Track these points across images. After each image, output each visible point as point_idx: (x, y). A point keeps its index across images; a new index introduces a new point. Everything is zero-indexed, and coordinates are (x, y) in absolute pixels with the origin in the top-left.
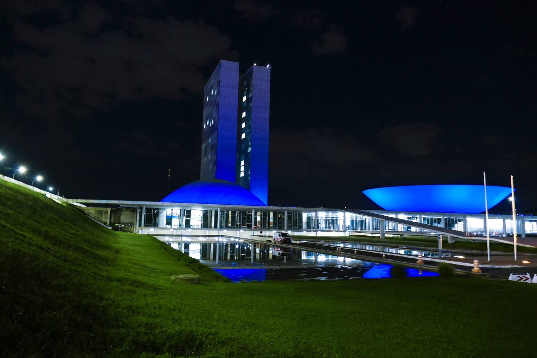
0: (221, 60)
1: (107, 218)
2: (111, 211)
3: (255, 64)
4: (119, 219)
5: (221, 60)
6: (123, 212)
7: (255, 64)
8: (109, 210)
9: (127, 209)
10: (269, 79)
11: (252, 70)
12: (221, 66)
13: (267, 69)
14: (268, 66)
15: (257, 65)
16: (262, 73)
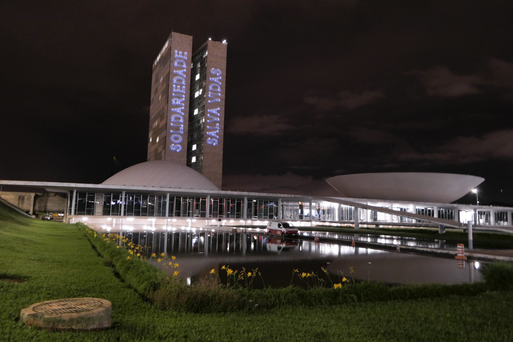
0: (173, 33)
1: (30, 205)
2: (36, 197)
4: (46, 206)
5: (173, 33)
6: (50, 198)
7: (210, 39)
8: (33, 195)
9: (56, 194)
10: (226, 56)
11: (207, 46)
12: (173, 39)
13: (223, 45)
14: (224, 42)
15: (212, 40)
16: (217, 50)
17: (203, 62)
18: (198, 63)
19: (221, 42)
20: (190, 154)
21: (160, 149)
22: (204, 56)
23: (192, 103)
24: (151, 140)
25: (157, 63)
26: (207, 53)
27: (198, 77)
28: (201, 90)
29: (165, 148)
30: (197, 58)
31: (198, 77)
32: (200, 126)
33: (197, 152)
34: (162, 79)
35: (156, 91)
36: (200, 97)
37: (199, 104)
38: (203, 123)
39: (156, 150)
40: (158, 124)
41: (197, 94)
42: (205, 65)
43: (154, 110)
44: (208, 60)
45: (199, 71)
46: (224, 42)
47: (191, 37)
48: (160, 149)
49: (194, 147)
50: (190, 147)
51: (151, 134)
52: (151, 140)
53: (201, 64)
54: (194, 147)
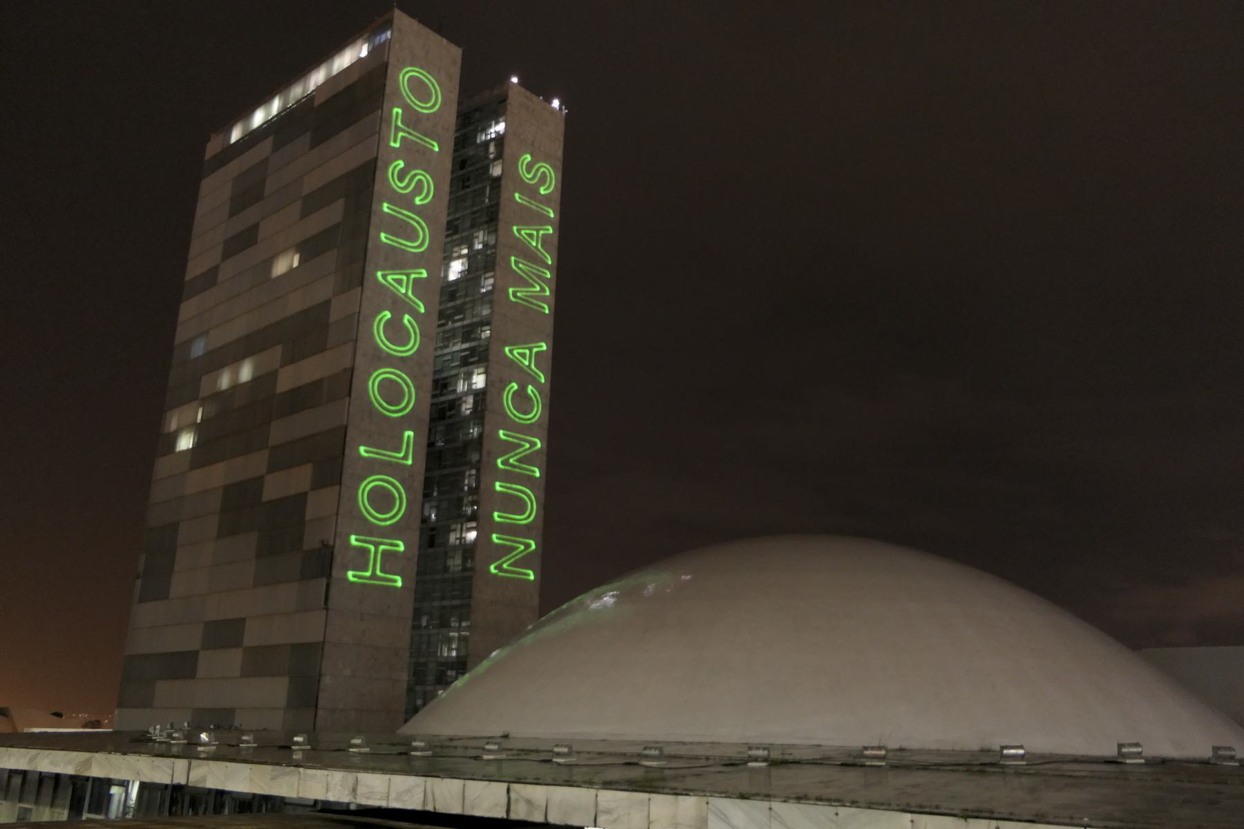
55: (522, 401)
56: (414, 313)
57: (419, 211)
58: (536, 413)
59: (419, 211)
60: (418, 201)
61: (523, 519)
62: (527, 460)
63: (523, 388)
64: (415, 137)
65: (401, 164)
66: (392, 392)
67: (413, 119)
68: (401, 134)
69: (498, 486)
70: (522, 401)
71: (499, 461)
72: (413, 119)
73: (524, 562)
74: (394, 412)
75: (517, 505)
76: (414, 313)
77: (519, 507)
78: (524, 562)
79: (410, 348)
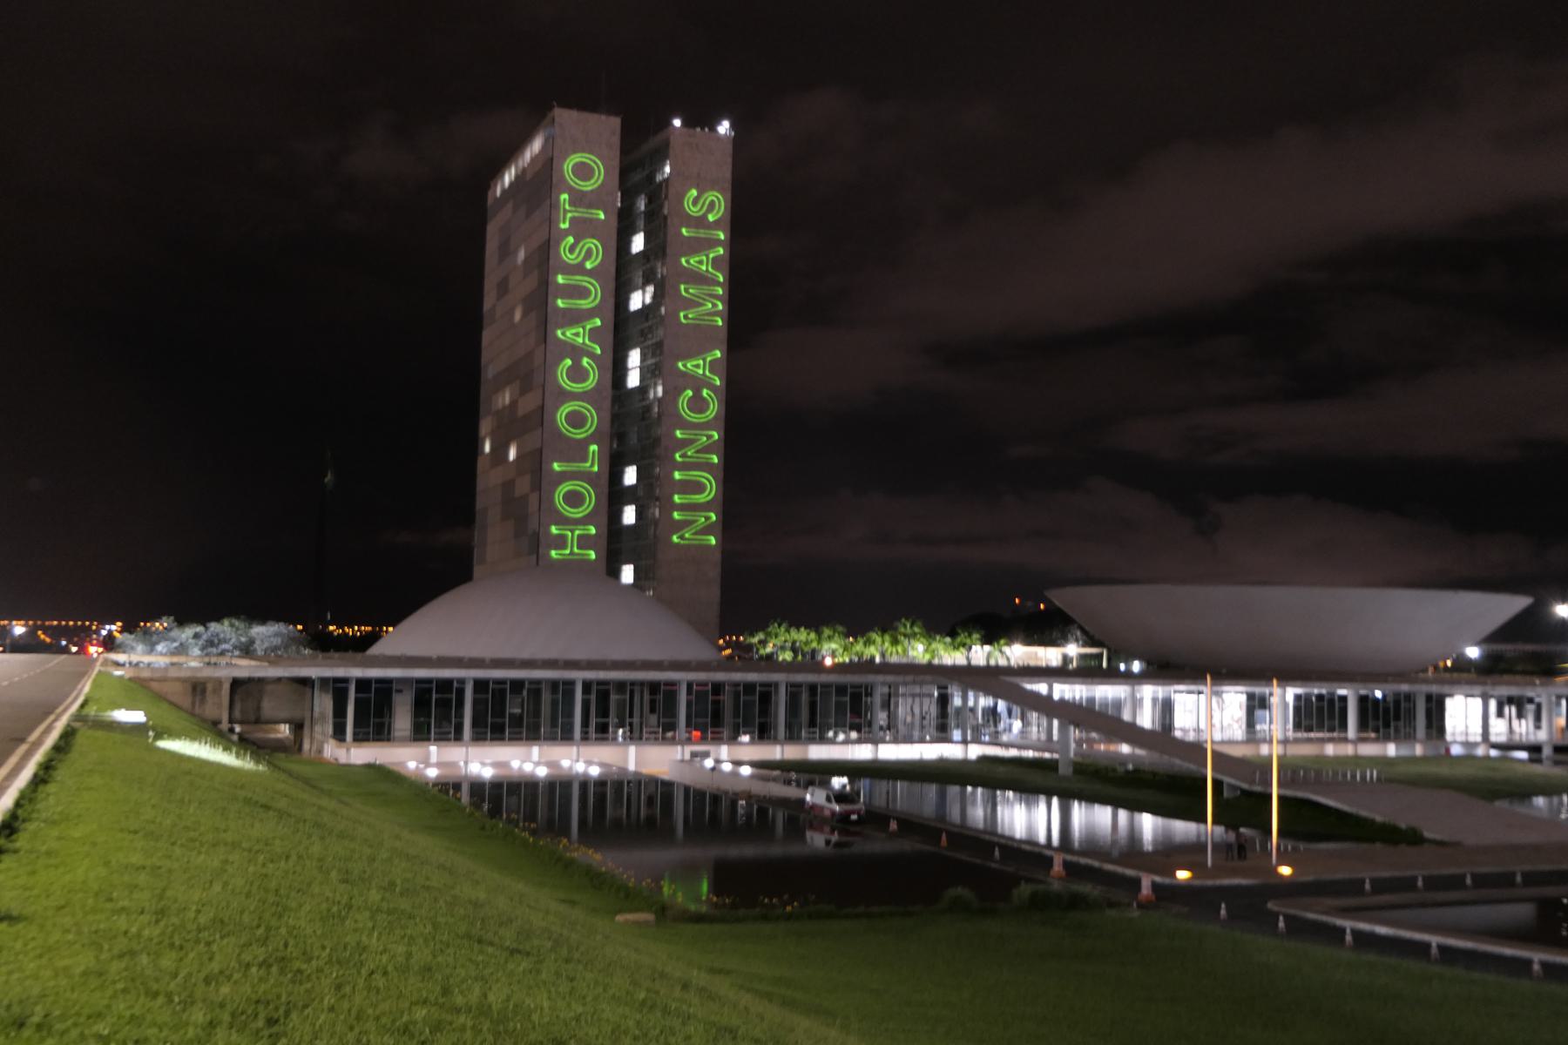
3: (677, 123)
14: (724, 128)
17: (657, 194)
18: (637, 194)
19: (713, 129)
20: (616, 496)
21: (523, 485)
22: (659, 178)
23: (623, 330)
24: (487, 448)
25: (504, 191)
26: (667, 169)
27: (638, 243)
28: (650, 289)
29: (537, 486)
30: (637, 177)
31: (638, 243)
32: (648, 409)
33: (641, 493)
34: (521, 255)
35: (503, 288)
36: (645, 308)
37: (644, 334)
38: (660, 400)
39: (508, 485)
40: (514, 403)
41: (637, 301)
42: (661, 206)
43: (496, 350)
44: (672, 191)
45: (641, 223)
46: (724, 128)
47: (615, 122)
48: (523, 485)
49: (630, 476)
50: (616, 475)
51: (485, 426)
52: (487, 448)
53: (650, 202)
54: (630, 476)
55: (698, 404)
56: (591, 355)
57: (590, 273)
58: (713, 409)
59: (590, 273)
60: (588, 265)
61: (701, 498)
62: (707, 449)
63: (697, 392)
64: (581, 213)
65: (571, 240)
66: (576, 420)
67: (578, 199)
68: (569, 215)
69: (677, 475)
70: (698, 404)
71: (677, 456)
72: (578, 199)
73: (707, 530)
74: (579, 434)
75: (698, 488)
76: (591, 355)
77: (698, 488)
78: (707, 530)
79: (591, 382)
